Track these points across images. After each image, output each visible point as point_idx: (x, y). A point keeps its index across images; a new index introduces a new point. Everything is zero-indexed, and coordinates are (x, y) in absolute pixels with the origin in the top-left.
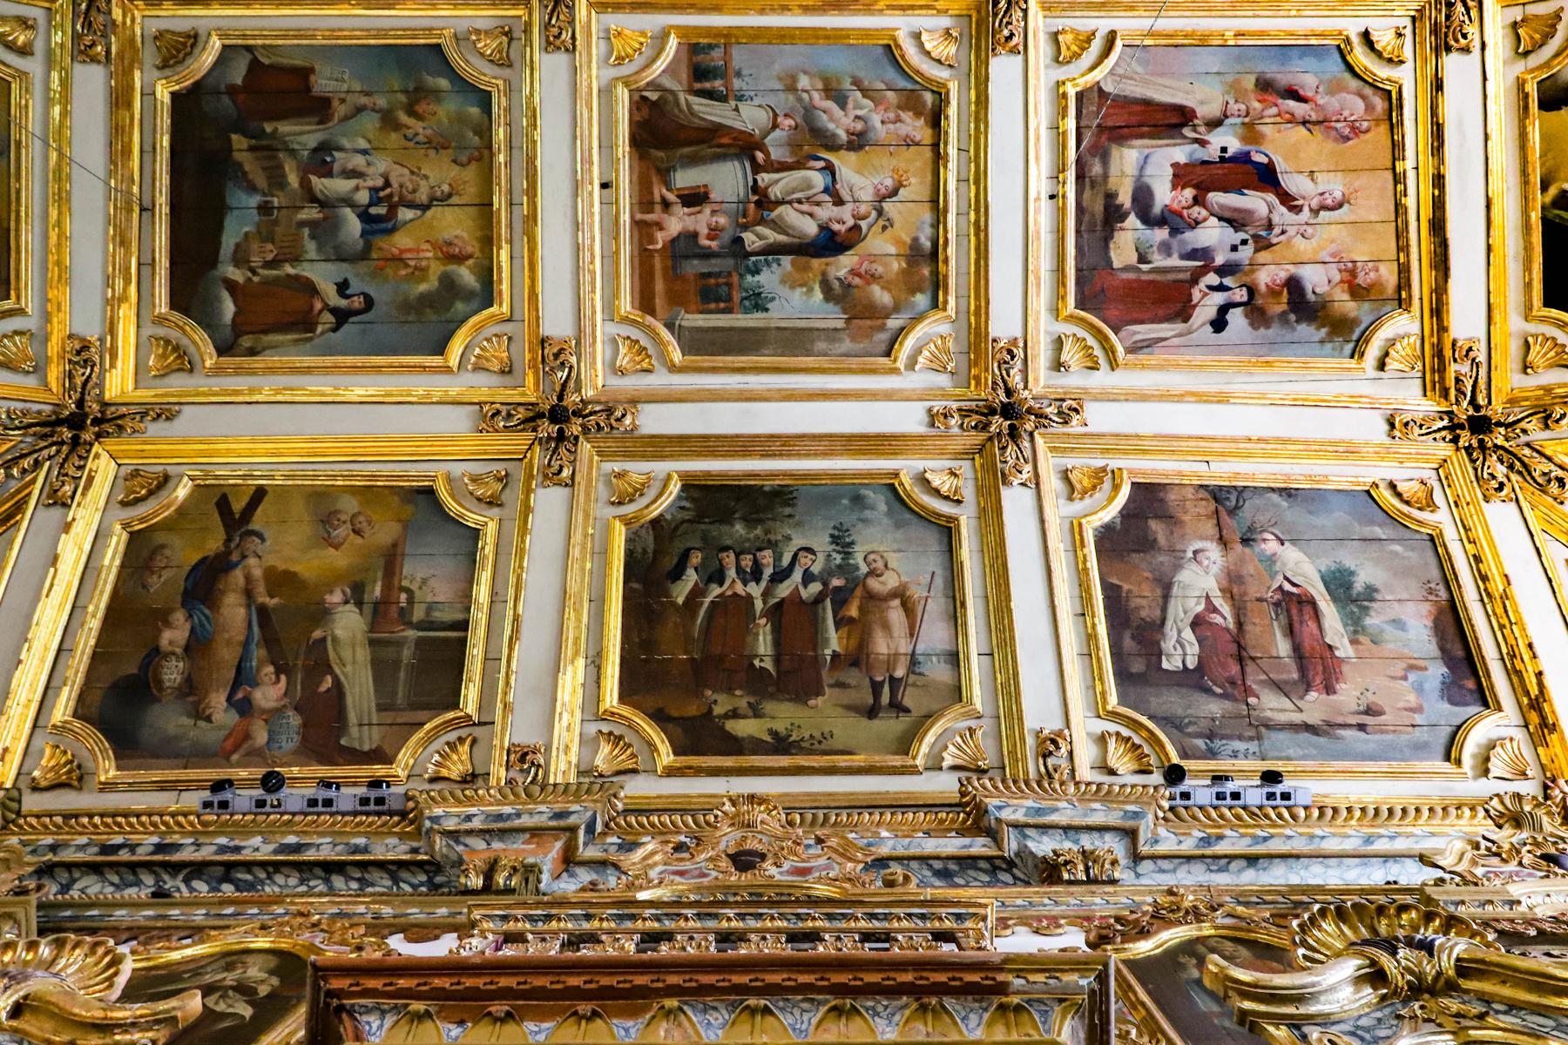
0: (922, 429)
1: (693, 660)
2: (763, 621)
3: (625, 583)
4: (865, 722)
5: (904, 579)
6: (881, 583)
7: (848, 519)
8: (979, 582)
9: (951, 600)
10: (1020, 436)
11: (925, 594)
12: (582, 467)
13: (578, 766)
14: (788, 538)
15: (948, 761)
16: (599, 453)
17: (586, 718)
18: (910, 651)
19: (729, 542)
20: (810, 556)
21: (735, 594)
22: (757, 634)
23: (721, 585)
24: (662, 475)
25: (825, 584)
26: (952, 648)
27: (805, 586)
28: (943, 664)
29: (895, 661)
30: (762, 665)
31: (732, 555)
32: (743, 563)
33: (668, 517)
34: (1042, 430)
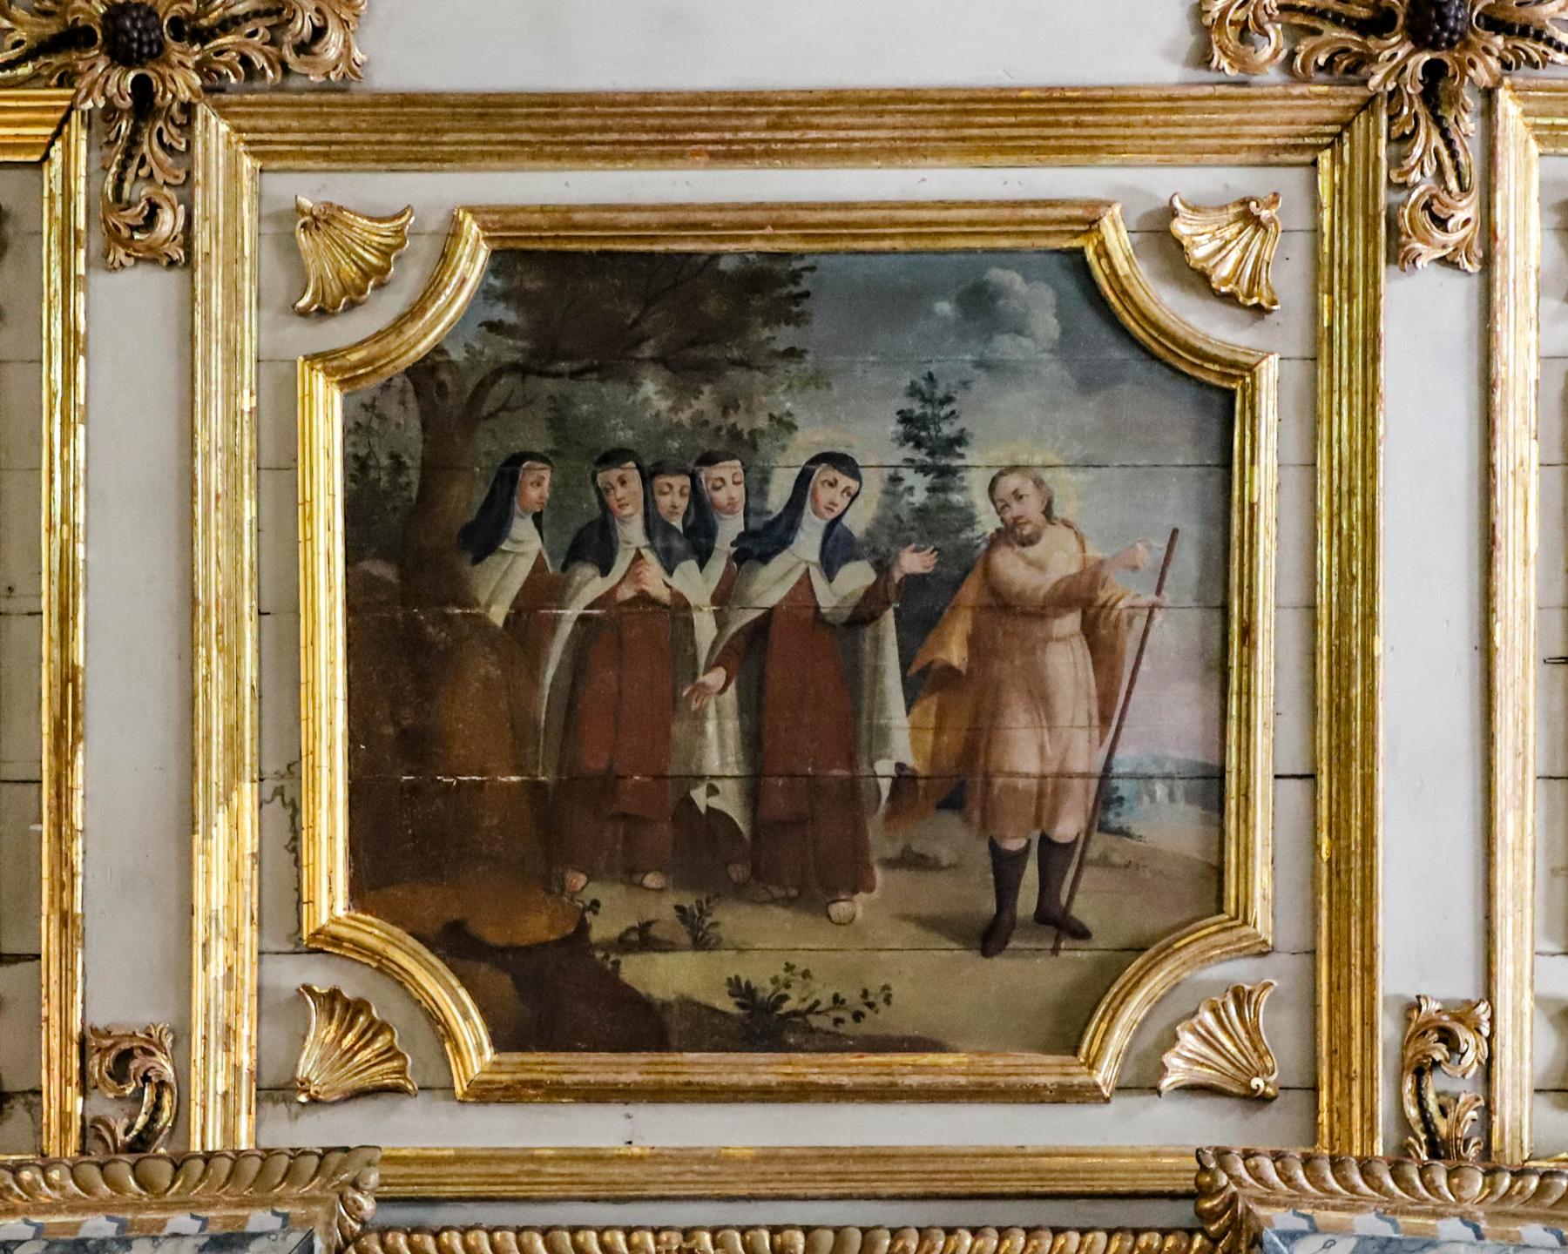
0: (1170, 73)
1: (535, 788)
2: (716, 678)
3: (349, 562)
4: (971, 963)
5: (1094, 552)
7: (951, 363)
9: (1217, 615)
10: (1454, 99)
11: (1150, 598)
12: (210, 200)
13: (256, 1075)
14: (786, 425)
17: (271, 946)
18: (1098, 768)
19: (625, 436)
20: (845, 481)
21: (643, 598)
22: (700, 716)
23: (605, 570)
24: (435, 221)
25: (882, 567)
27: (830, 573)
28: (1181, 806)
29: (1056, 792)
30: (715, 802)
31: (631, 471)
32: (664, 502)
33: (457, 355)
34: (1521, 76)
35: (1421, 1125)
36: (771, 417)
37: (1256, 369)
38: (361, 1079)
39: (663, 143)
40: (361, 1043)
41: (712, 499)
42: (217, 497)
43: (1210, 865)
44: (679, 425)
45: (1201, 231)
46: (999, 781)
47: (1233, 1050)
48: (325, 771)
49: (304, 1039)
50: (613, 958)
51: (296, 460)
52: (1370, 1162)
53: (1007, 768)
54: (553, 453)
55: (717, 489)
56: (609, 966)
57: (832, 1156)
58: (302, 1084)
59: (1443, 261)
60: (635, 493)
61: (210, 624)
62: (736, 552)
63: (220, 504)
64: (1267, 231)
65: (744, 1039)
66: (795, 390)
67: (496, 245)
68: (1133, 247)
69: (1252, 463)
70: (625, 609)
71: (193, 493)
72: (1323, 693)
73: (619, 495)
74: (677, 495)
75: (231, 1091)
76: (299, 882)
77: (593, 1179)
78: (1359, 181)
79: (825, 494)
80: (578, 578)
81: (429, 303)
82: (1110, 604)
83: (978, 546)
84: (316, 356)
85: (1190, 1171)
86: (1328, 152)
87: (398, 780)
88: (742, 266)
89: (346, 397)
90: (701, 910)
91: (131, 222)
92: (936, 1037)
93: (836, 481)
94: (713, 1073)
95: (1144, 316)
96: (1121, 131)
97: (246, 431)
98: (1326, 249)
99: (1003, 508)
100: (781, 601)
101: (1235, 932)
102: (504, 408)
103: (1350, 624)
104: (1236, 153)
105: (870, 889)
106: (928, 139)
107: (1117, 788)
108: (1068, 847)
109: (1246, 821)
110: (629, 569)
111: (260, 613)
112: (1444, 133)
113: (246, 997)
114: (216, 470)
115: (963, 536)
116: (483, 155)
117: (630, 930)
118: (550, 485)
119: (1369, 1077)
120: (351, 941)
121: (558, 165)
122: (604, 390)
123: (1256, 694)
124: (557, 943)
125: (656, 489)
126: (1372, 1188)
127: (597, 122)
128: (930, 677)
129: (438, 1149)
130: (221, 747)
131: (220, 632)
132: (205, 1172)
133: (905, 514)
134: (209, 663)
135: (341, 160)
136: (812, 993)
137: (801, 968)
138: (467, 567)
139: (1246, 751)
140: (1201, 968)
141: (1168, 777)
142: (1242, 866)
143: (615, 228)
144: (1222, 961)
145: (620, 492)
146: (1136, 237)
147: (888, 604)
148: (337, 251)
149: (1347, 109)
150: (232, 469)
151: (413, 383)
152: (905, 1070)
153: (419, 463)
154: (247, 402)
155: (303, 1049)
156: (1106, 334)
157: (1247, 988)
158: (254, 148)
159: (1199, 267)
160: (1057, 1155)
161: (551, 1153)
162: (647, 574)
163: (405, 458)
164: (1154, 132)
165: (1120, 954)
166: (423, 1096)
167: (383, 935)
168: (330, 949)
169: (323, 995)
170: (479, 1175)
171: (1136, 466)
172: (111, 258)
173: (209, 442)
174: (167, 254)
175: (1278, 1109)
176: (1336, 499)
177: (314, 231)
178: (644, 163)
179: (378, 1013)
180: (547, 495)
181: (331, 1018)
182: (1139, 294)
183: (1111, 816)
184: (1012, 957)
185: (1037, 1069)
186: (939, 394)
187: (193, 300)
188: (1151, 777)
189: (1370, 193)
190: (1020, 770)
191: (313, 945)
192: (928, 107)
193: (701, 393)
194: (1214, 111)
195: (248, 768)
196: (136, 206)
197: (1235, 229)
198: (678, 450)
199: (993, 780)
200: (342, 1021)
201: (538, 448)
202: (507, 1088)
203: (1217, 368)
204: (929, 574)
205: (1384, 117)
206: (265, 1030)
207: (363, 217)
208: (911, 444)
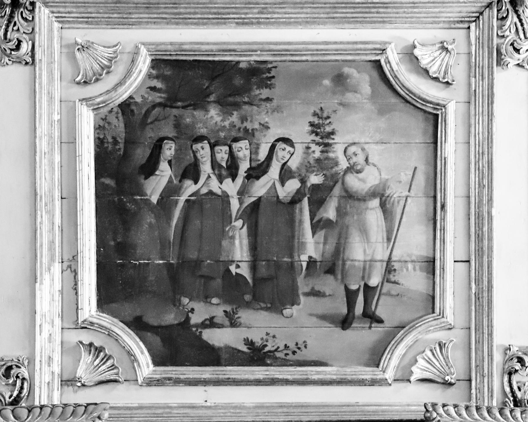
1: (169, 266)
2: (239, 223)
3: (97, 178)
5: (384, 176)
8: (461, 181)
9: (431, 200)
11: (407, 193)
12: (41, 39)
14: (266, 127)
15: (417, 373)
16: (61, 20)
17: (66, 325)
18: (386, 258)
19: (203, 131)
20: (289, 148)
21: (211, 193)
22: (233, 238)
23: (196, 182)
24: (129, 48)
25: (303, 181)
26: (431, 256)
27: (283, 184)
28: (418, 273)
30: (239, 271)
35: (511, 394)
36: (260, 124)
39: (218, 18)
43: (430, 295)
44: (224, 127)
46: (348, 263)
47: (439, 366)
48: (87, 258)
49: (79, 361)
50: (199, 330)
51: (75, 139)
52: (491, 408)
53: (351, 258)
54: (175, 137)
55: (239, 151)
56: (198, 334)
57: (284, 406)
58: (79, 379)
59: (518, 65)
60: (207, 153)
61: (42, 202)
62: (247, 176)
63: (46, 156)
66: (269, 113)
67: (153, 57)
68: (399, 60)
69: (445, 142)
70: (203, 197)
71: (35, 152)
72: (473, 229)
73: (201, 154)
74: (224, 153)
75: (51, 382)
77: (192, 415)
78: (486, 35)
81: (127, 79)
82: (390, 196)
83: (340, 173)
84: (84, 99)
85: (422, 412)
86: (474, 23)
87: (116, 262)
88: (248, 66)
91: (11, 48)
92: (324, 361)
93: (285, 149)
94: (238, 375)
95: (403, 86)
96: (395, 15)
97: (56, 128)
98: (474, 61)
99: (349, 159)
101: (439, 320)
102: (156, 120)
103: (483, 204)
104: (438, 24)
105: (299, 304)
108: (374, 288)
109: (443, 278)
110: (205, 182)
111: (62, 198)
112: (519, 16)
113: (57, 346)
115: (334, 170)
116: (148, 23)
117: (206, 320)
119: (491, 375)
120: (97, 324)
121: (177, 27)
122: (195, 113)
124: (178, 324)
125: (216, 151)
126: (492, 418)
127: (192, 10)
128: (322, 223)
129: (132, 404)
131: (46, 205)
133: (312, 162)
134: (42, 217)
135: (93, 24)
136: (276, 344)
137: (271, 335)
138: (142, 181)
139: (443, 251)
141: (412, 261)
142: (442, 296)
143: (199, 51)
144: (434, 332)
145: (202, 152)
146: (401, 56)
148: (91, 59)
149: (482, 7)
150: (50, 143)
151: (121, 110)
152: (312, 373)
153: (124, 141)
154: (56, 117)
155: (79, 365)
157: (444, 342)
159: (424, 67)
160: (371, 406)
162: (212, 183)
163: (118, 139)
164: (407, 15)
165: (395, 329)
166: (125, 382)
167: (110, 322)
168: (89, 327)
169: (87, 345)
170: (148, 414)
171: (401, 143)
172: (3, 61)
173: (42, 132)
174: (25, 60)
175: (456, 388)
177: (82, 52)
178: (210, 26)
179: (108, 351)
180: (173, 153)
181: (90, 353)
182: (401, 78)
184: (354, 330)
185: (363, 373)
186: (325, 115)
187: (35, 78)
188: (406, 262)
189: (490, 39)
190: (355, 259)
191: (83, 326)
192: (320, 5)
193: (233, 114)
194: (430, 8)
195: (57, 258)
196: (13, 41)
197: (438, 52)
199: (346, 262)
201: (170, 136)
202: (158, 380)
203: (432, 106)
204: (321, 184)
206: (64, 358)
207: (101, 46)
208: (314, 134)
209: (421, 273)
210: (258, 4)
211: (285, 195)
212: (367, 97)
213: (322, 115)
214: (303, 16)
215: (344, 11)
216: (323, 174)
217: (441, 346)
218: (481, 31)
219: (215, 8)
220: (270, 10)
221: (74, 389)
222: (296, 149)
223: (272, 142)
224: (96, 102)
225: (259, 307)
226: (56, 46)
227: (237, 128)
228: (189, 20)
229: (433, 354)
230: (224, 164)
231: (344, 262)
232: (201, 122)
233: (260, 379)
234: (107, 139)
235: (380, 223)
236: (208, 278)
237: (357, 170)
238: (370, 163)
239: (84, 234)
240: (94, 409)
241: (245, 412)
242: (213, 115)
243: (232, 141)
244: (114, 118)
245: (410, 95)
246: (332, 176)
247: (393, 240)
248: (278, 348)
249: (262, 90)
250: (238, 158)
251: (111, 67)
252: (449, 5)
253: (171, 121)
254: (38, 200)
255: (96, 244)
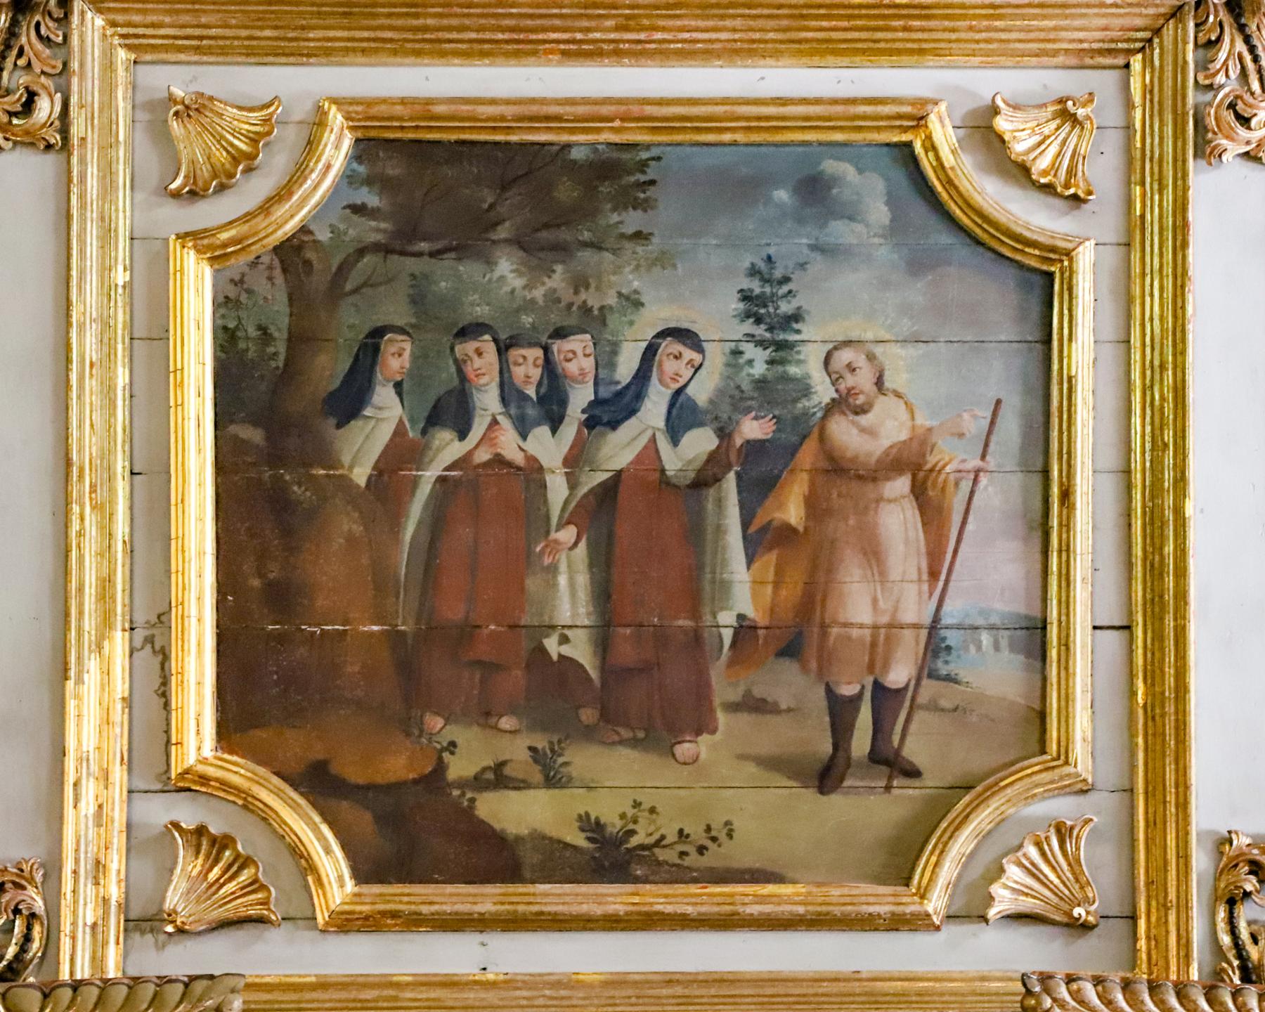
1: (395, 638)
5: (923, 420)
6: (863, 430)
9: (1037, 479)
11: (977, 463)
14: (633, 302)
15: (1004, 899)
18: (927, 619)
19: (481, 312)
20: (689, 354)
21: (499, 460)
22: (553, 569)
23: (463, 435)
24: (302, 111)
25: (724, 434)
26: (1037, 613)
27: (675, 441)
28: (1006, 653)
30: (566, 650)
32: (519, 372)
33: (323, 235)
35: (1234, 951)
36: (620, 294)
37: (1074, 253)
38: (228, 910)
40: (226, 876)
41: (563, 369)
42: (92, 365)
43: (1033, 709)
44: (533, 301)
45: (1022, 127)
46: (835, 631)
47: (1056, 881)
48: (194, 621)
49: (172, 871)
50: (469, 795)
52: (1185, 986)
53: (842, 619)
54: (413, 326)
55: (569, 360)
56: (466, 803)
57: (678, 981)
58: (169, 915)
60: (491, 364)
61: (84, 482)
62: (587, 420)
64: (1083, 128)
65: (594, 871)
67: (359, 134)
68: (958, 141)
69: (1070, 340)
72: (1138, 551)
73: (476, 366)
74: (531, 366)
75: (100, 922)
76: (168, 724)
77: (450, 1003)
78: (1169, 83)
79: (670, 366)
80: (437, 442)
81: (295, 187)
82: (937, 469)
83: (815, 413)
84: (187, 234)
85: (1019, 994)
86: (1139, 56)
87: (263, 629)
89: (217, 273)
90: (552, 751)
91: (9, 109)
92: (777, 870)
93: (680, 354)
94: (563, 904)
95: (969, 205)
97: (120, 304)
98: (1138, 145)
99: (837, 379)
100: (631, 463)
101: (1056, 771)
102: (365, 285)
103: (1163, 489)
104: (1054, 56)
105: (713, 731)
106: (766, 42)
107: (944, 639)
108: (900, 692)
109: (1067, 669)
110: (485, 434)
111: (132, 473)
112: (1247, 40)
113: (116, 833)
114: (91, 339)
115: (800, 405)
117: (485, 769)
118: (411, 355)
120: (217, 780)
121: (419, 60)
122: (461, 268)
123: (1075, 552)
124: (416, 782)
125: (511, 360)
127: (454, 22)
128: (769, 536)
129: (300, 976)
130: (93, 599)
131: (93, 489)
132: (73, 999)
135: (212, 54)
137: (646, 806)
139: (1066, 604)
140: (1025, 805)
141: (992, 628)
142: (1064, 712)
144: (1044, 799)
145: (478, 363)
146: (961, 132)
147: (729, 467)
150: (106, 340)
151: (282, 262)
152: (747, 900)
153: (285, 336)
154: (121, 277)
155: (170, 881)
156: (933, 220)
157: (1069, 823)
158: (127, 42)
159: (1020, 159)
160: (890, 979)
161: (410, 979)
162: (502, 438)
163: (272, 330)
164: (977, 36)
165: (949, 791)
166: (284, 924)
167: (249, 774)
168: (198, 788)
169: (189, 831)
170: (340, 1001)
173: (84, 314)
175: (1099, 936)
176: (1148, 373)
177: (186, 119)
178: (500, 60)
179: (243, 848)
180: (407, 365)
181: (198, 853)
182: (964, 185)
183: (940, 664)
184: (847, 793)
185: (871, 900)
186: (778, 274)
187: (70, 180)
188: (977, 628)
189: (1179, 94)
190: (853, 621)
191: (181, 784)
192: (766, 11)
193: (554, 271)
194: (1035, 17)
195: (119, 618)
196: (15, 94)
197: (1053, 125)
198: (533, 325)
199: (829, 630)
200: (207, 857)
201: (400, 322)
202: (366, 918)
203: (1037, 252)
204: (767, 440)
205: (1191, 25)
206: (133, 863)
207: (233, 106)
208: (751, 320)
209: (1012, 656)
210: (616, 8)
211: (679, 466)
212: (881, 232)
213: (771, 274)
214: (724, 36)
215: (825, 24)
216: (774, 417)
217: (1063, 832)
218: (1157, 74)
219: (511, 15)
220: (646, 22)
221: (156, 941)
222: (706, 353)
223: (650, 338)
224: (218, 242)
225: (616, 738)
226: (121, 104)
227: (563, 304)
228: (447, 46)
229: (1043, 854)
230: (531, 392)
231: (824, 627)
232: (475, 291)
233: (617, 915)
234: (246, 331)
235: (911, 534)
236: (490, 668)
237: (856, 406)
238: (888, 390)
239: (187, 560)
240: (208, 990)
241: (581, 995)
242: (506, 273)
243: (550, 337)
244: (264, 281)
245: (985, 226)
246: (796, 419)
247: (943, 577)
248: (663, 837)
249: (624, 214)
250: (566, 377)
251: (258, 155)
252: (1079, 11)
253: (402, 289)
254: (75, 479)
255: (215, 585)
